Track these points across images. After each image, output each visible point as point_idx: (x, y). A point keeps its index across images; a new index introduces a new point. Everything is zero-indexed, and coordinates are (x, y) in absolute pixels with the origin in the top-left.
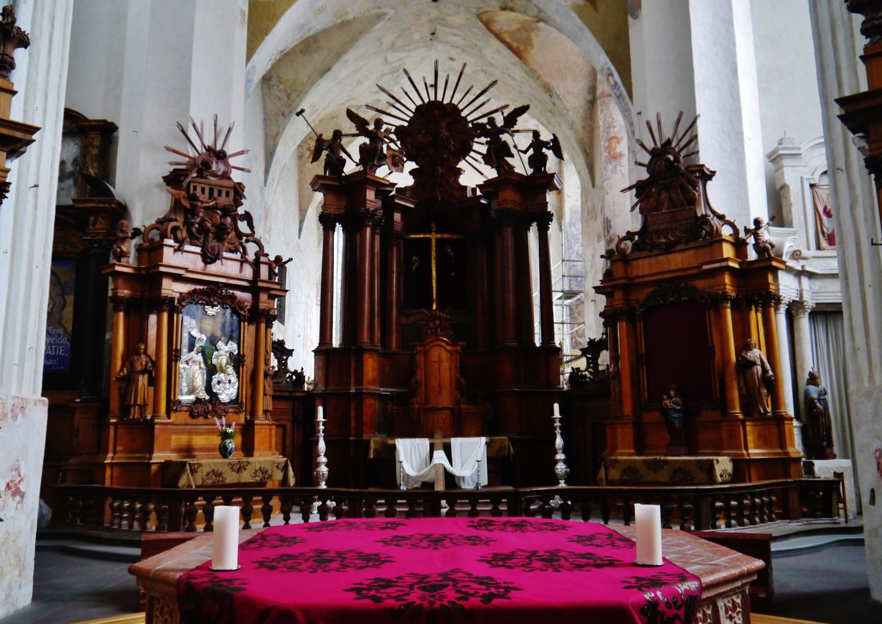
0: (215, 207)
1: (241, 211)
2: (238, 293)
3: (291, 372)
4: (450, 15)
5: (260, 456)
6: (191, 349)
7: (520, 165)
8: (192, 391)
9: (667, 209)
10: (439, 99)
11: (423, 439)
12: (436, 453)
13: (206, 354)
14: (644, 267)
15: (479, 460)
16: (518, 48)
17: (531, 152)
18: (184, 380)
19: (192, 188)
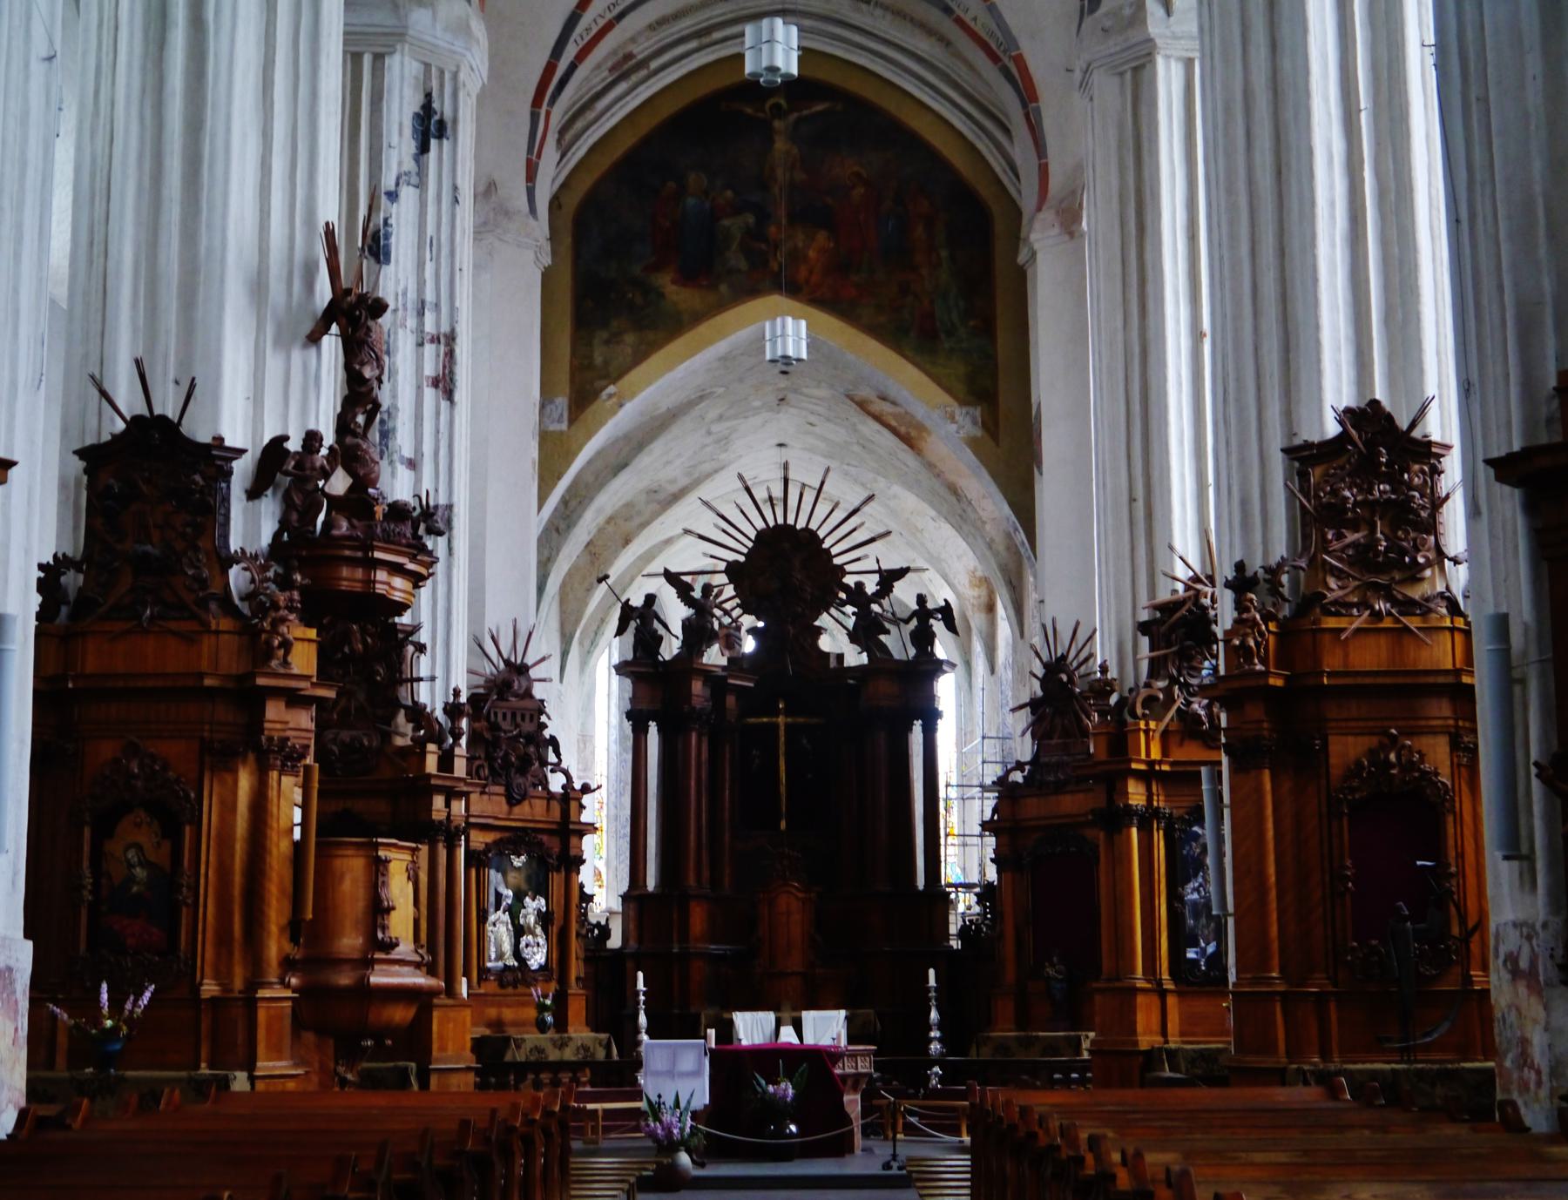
0: (519, 735)
1: (547, 733)
2: (545, 838)
3: (590, 924)
4: (807, 387)
5: (575, 1031)
6: (497, 908)
7: (897, 643)
8: (500, 956)
9: (1059, 738)
10: (791, 521)
11: (767, 1013)
12: (783, 1029)
13: (514, 912)
14: (1033, 808)
15: (835, 1036)
16: (908, 433)
17: (914, 622)
18: (492, 944)
19: (492, 715)
